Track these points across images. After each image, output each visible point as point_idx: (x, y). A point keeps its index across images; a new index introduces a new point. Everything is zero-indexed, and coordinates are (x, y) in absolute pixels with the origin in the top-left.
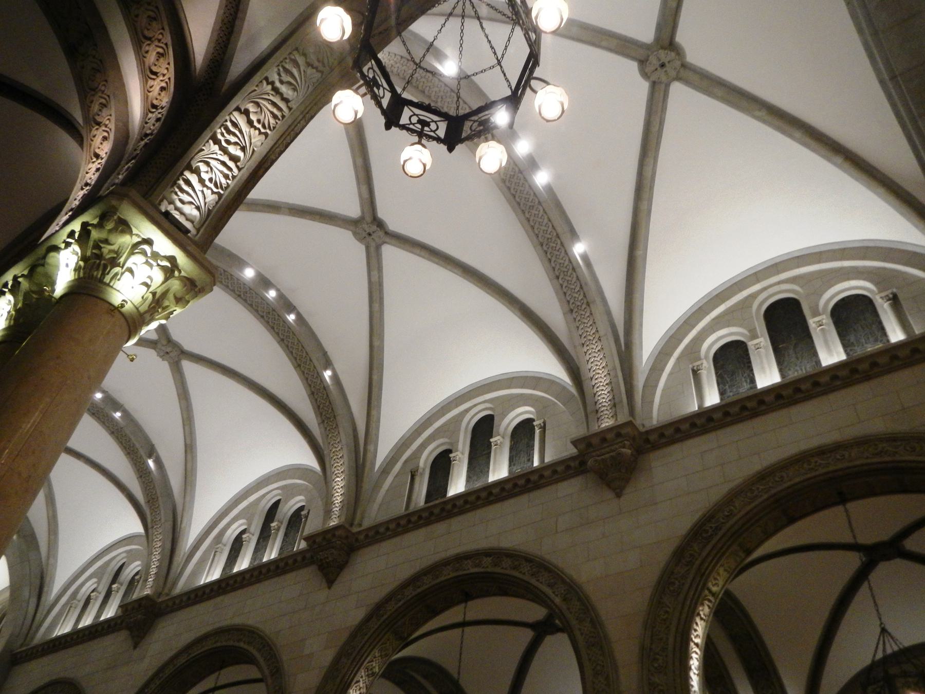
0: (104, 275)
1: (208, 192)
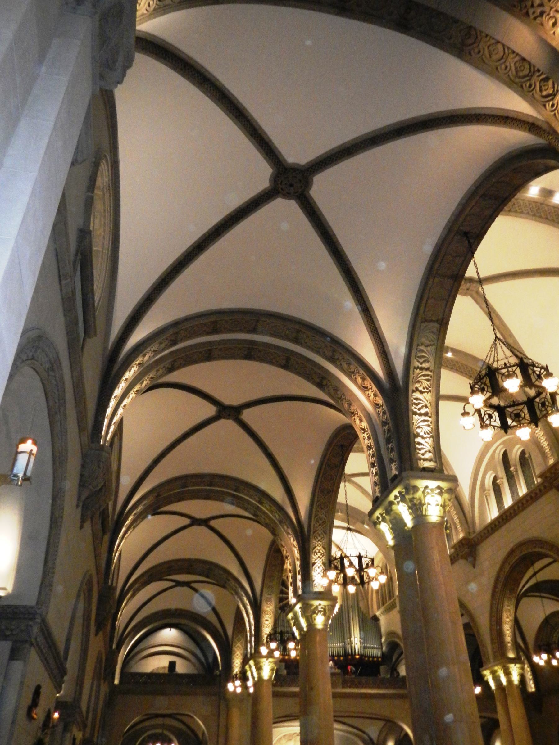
0: (422, 512)
1: (427, 440)
